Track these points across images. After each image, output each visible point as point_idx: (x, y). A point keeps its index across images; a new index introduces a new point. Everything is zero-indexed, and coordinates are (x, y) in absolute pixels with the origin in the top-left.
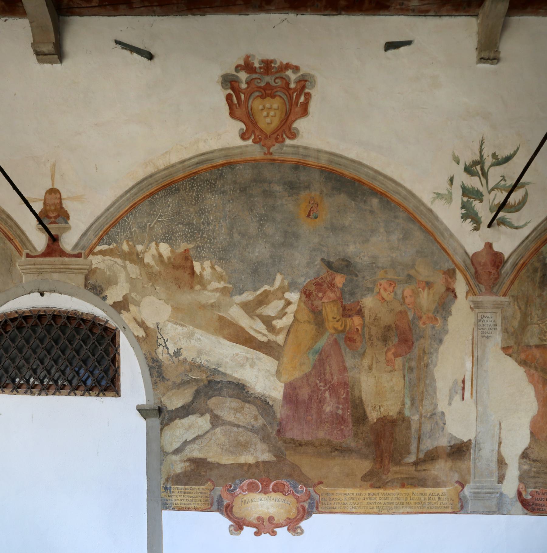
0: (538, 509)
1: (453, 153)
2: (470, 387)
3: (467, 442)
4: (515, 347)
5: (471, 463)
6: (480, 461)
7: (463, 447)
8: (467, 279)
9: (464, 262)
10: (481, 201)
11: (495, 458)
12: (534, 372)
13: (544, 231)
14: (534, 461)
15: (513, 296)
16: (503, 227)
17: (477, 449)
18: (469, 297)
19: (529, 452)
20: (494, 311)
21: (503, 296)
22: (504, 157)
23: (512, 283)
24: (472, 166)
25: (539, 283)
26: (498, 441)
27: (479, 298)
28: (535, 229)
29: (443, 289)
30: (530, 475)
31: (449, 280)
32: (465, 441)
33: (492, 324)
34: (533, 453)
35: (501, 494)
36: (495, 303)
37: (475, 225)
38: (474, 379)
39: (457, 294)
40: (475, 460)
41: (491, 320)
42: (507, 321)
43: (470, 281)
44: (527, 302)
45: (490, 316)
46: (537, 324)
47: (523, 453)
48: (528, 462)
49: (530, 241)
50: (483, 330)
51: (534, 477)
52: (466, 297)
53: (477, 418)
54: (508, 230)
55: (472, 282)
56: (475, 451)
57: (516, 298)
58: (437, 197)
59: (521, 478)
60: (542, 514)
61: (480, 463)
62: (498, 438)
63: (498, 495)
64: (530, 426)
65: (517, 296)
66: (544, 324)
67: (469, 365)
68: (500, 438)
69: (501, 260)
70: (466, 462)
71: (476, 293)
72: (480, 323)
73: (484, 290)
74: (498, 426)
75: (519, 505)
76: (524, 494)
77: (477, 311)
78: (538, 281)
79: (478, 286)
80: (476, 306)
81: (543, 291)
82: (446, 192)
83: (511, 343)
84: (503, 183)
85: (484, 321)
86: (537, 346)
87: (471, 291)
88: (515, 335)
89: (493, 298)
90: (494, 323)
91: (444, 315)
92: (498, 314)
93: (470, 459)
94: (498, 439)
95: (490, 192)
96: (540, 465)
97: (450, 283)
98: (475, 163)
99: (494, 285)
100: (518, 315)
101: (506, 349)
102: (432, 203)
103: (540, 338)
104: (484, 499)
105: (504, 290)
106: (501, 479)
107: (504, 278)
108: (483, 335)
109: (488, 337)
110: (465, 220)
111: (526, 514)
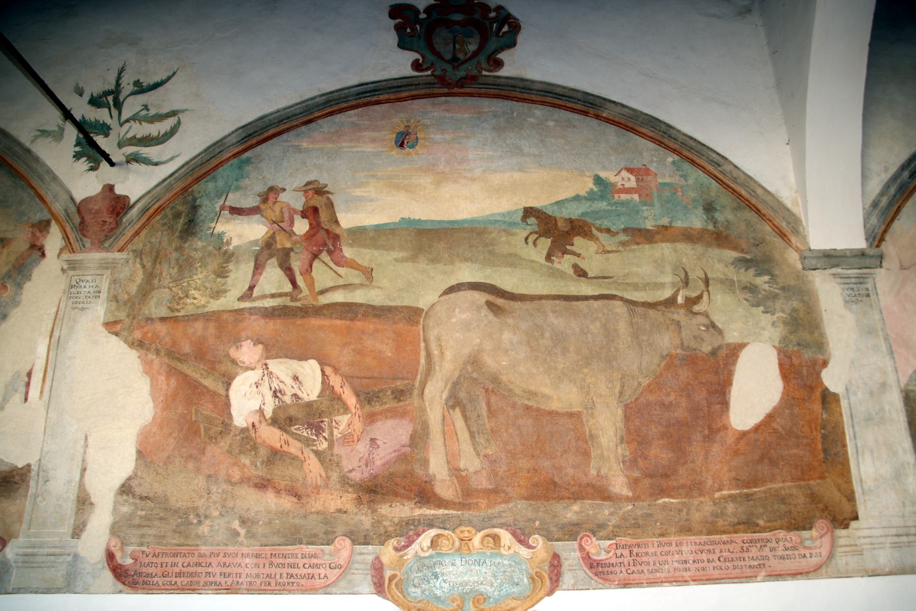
0: (145, 583)
1: (77, 84)
2: (41, 382)
3: (22, 469)
4: (127, 321)
5: (27, 502)
6: (44, 499)
7: (13, 477)
8: (65, 232)
9: (66, 211)
10: (107, 135)
11: (73, 495)
12: (154, 357)
13: (201, 165)
14: (141, 498)
15: (134, 251)
16: (135, 164)
17: (41, 480)
18: (63, 255)
19: (134, 483)
20: (99, 272)
21: (119, 251)
22: (152, 83)
23: (137, 233)
24: (101, 97)
25: (181, 232)
26: (80, 466)
27: (78, 257)
28: (187, 163)
29: (27, 246)
30: (133, 522)
31: (38, 234)
32: (20, 466)
33: (92, 290)
34: (141, 485)
35: (76, 556)
36: (102, 262)
37: (92, 164)
38: (49, 370)
39: (47, 252)
40: (36, 496)
41: (91, 284)
42: (118, 285)
43: (69, 234)
44: (157, 257)
45: (90, 280)
46: (169, 288)
47: (123, 485)
48: (131, 501)
49: (176, 178)
50: (76, 300)
51: (140, 526)
52: (59, 256)
53: (45, 430)
54: (143, 167)
55: (72, 236)
56: (37, 482)
57: (139, 254)
58: (41, 136)
59: (115, 530)
60: (151, 592)
61: (45, 503)
62: (80, 460)
63: (70, 558)
64: (137, 442)
65: (141, 251)
66: (180, 287)
67: (42, 350)
68: (84, 461)
69: (125, 205)
70: (18, 502)
71: (75, 249)
72: (73, 290)
73: (88, 245)
74: (83, 442)
75: (108, 575)
76: (118, 555)
77: (71, 273)
78: (179, 229)
79: (81, 240)
80: (73, 266)
81: (185, 242)
82: (56, 129)
83: (122, 315)
84: (144, 112)
85: (81, 287)
86: (163, 319)
87: (69, 246)
88: (129, 304)
89: (104, 255)
90: (97, 289)
91: (18, 280)
92: (105, 277)
93: (26, 496)
94: (80, 463)
95: (121, 125)
96: (153, 505)
97: (38, 239)
98: (106, 93)
99: (107, 237)
100: (140, 276)
101: (111, 326)
102: (32, 142)
103: (169, 308)
104: (42, 565)
105: (121, 243)
106: (78, 531)
107: (125, 228)
108: (75, 305)
109: (83, 309)
110: (79, 159)
111: (120, 592)
